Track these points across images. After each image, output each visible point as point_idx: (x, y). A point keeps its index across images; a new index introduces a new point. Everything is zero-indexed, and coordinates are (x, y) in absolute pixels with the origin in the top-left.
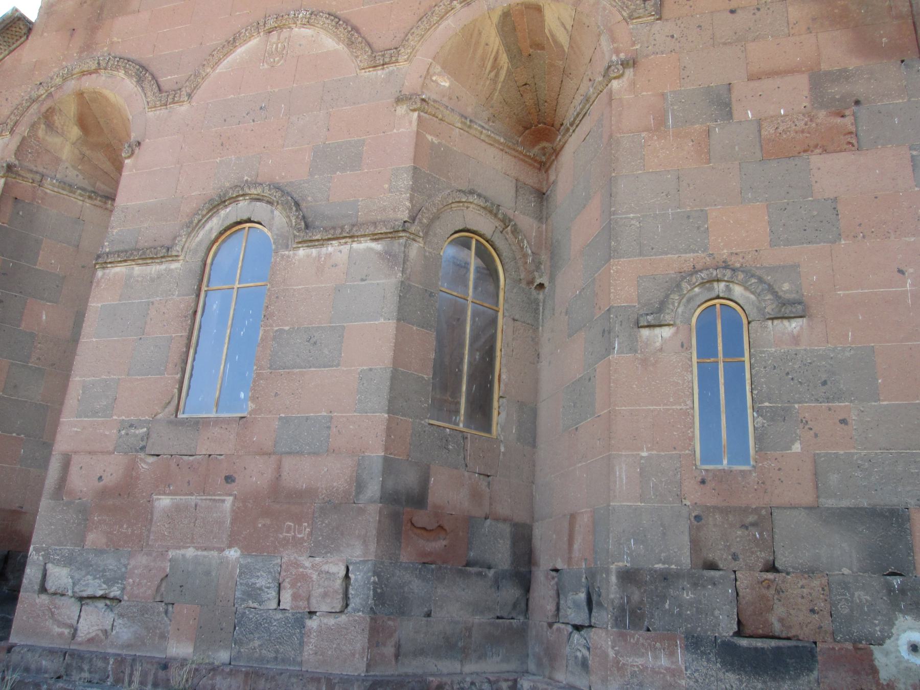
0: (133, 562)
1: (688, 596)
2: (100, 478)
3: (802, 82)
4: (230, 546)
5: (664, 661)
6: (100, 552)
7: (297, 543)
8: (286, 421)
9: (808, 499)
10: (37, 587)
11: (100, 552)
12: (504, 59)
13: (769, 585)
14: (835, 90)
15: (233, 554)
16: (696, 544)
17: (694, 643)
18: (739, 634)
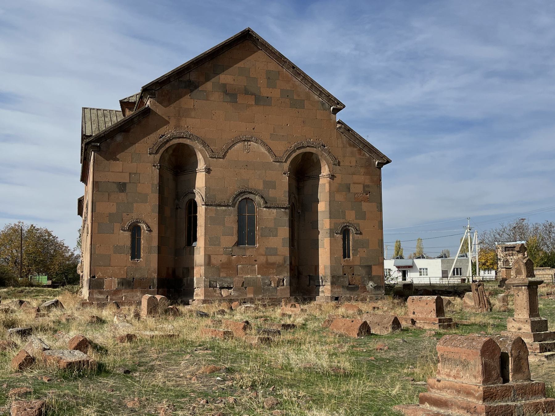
0: (234, 279)
1: (342, 280)
2: (221, 261)
3: (362, 186)
4: (258, 275)
5: (339, 290)
6: (225, 277)
7: (273, 273)
8: (267, 248)
9: (359, 264)
10: (209, 286)
11: (225, 277)
12: (300, 160)
13: (353, 277)
14: (367, 189)
15: (259, 276)
16: (343, 272)
17: (343, 287)
18: (349, 284)
